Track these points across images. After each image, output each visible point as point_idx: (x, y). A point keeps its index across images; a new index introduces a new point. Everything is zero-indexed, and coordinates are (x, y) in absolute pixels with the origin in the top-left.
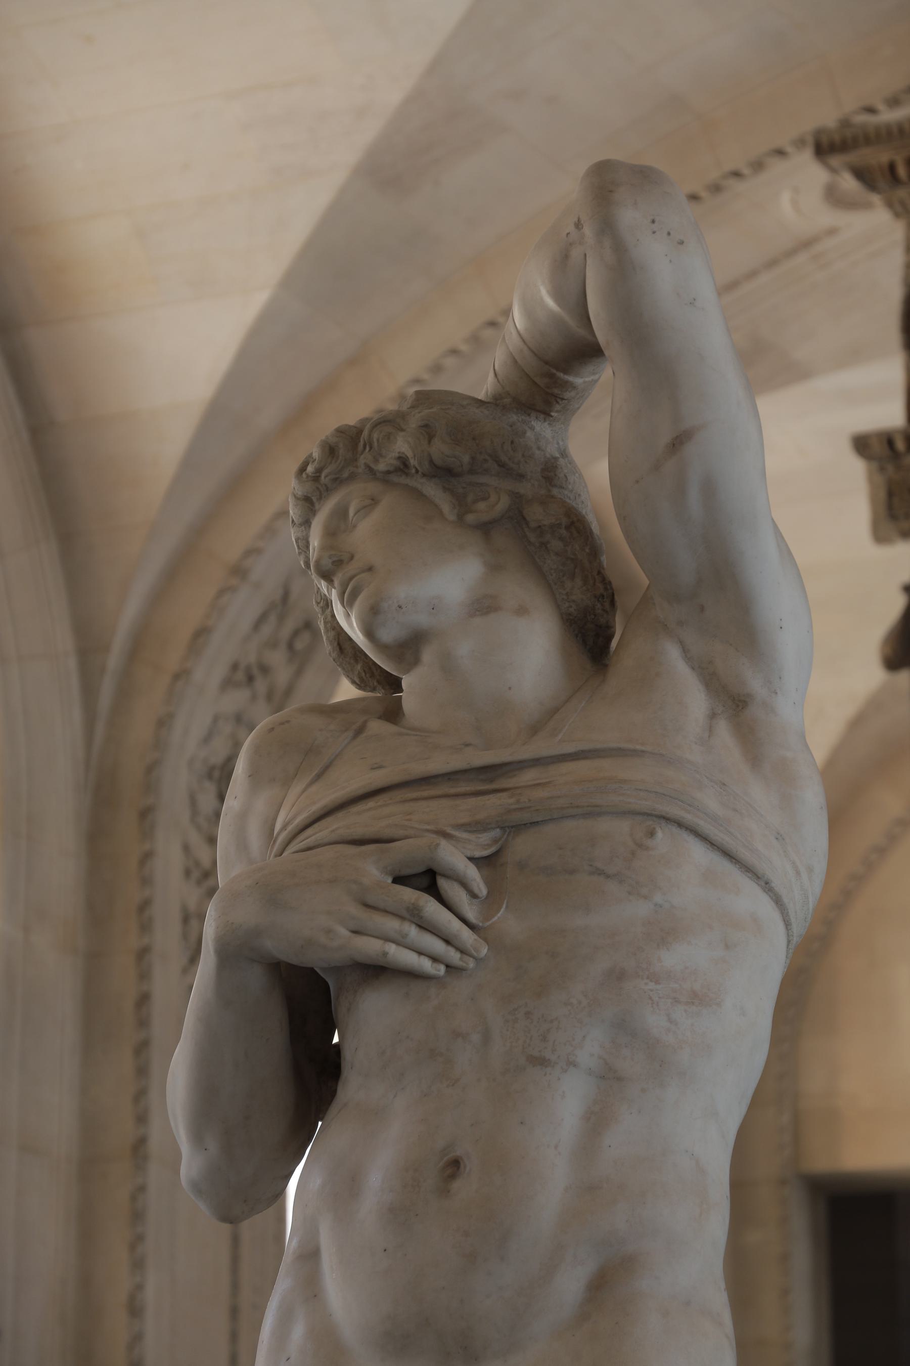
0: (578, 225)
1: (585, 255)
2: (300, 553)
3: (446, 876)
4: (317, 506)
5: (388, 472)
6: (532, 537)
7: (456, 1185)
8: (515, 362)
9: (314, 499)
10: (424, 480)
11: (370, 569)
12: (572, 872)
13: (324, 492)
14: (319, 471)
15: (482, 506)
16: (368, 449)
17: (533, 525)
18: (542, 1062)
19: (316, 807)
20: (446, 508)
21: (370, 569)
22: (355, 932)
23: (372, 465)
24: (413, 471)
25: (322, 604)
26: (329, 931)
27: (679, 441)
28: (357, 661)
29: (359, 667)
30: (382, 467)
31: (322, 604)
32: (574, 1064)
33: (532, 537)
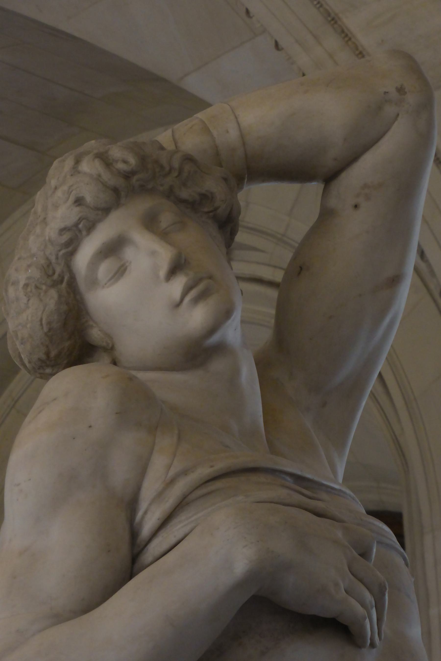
0: (401, 90)
1: (398, 115)
2: (62, 231)
8: (217, 154)
9: (123, 194)
11: (210, 277)
14: (133, 173)
21: (210, 277)
22: (346, 591)
24: (206, 210)
25: (56, 277)
26: (336, 585)
27: (395, 281)
29: (67, 344)
30: (184, 194)
31: (56, 277)
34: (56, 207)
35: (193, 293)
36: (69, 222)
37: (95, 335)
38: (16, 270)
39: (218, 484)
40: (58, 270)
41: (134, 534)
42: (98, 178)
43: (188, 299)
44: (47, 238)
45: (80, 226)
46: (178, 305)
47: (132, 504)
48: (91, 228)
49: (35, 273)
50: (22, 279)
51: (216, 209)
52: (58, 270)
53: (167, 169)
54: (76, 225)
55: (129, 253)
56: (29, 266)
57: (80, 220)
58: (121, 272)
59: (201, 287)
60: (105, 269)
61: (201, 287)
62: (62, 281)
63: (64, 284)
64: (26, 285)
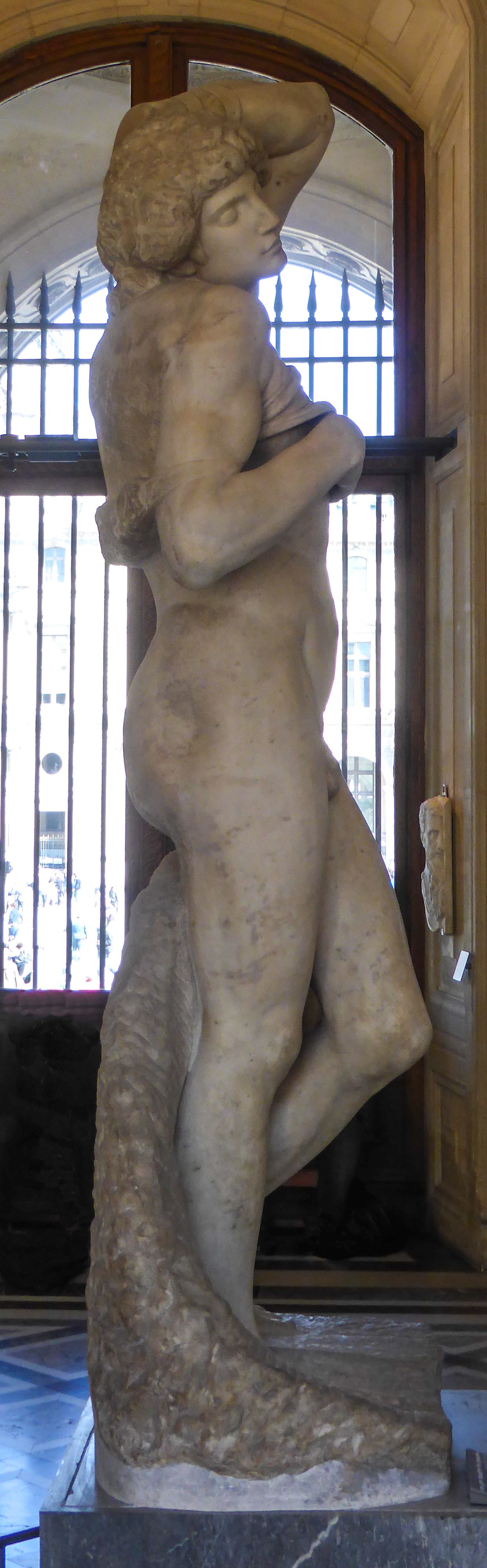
34: (209, 162)
36: (218, 178)
38: (165, 195)
40: (197, 205)
42: (240, 152)
44: (198, 182)
45: (224, 182)
49: (184, 203)
50: (172, 203)
52: (197, 205)
54: (222, 180)
55: (242, 208)
56: (179, 197)
60: (226, 215)
64: (174, 209)
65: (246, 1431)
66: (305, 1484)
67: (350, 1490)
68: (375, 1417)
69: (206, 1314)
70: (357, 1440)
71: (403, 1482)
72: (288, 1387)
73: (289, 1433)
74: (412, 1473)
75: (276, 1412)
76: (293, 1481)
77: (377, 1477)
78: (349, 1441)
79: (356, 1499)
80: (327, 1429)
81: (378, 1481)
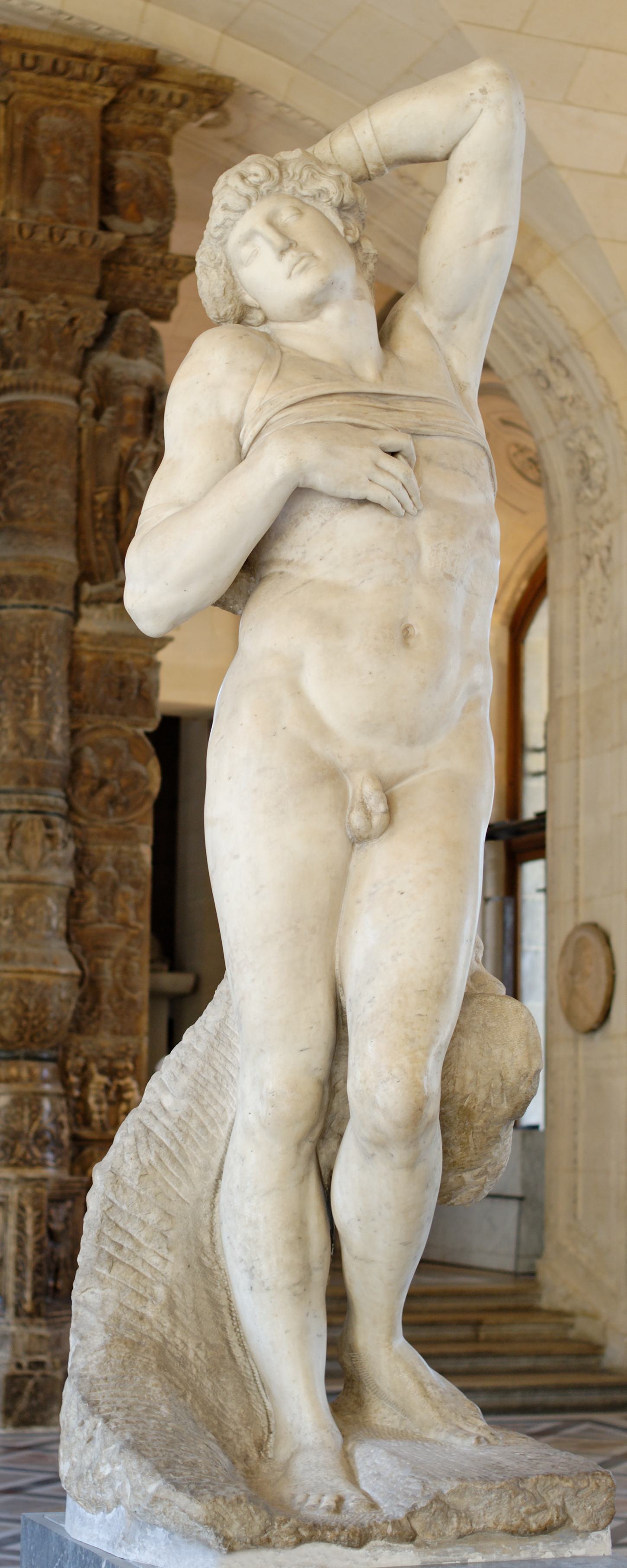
3: (405, 457)
4: (254, 203)
5: (305, 196)
6: (361, 258)
7: (412, 641)
8: (360, 149)
9: (253, 199)
10: (329, 208)
12: (456, 470)
13: (259, 196)
15: (351, 232)
16: (297, 178)
17: (365, 251)
18: (450, 577)
19: (300, 397)
20: (341, 229)
23: (298, 189)
24: (325, 200)
25: (216, 261)
28: (230, 303)
29: (230, 307)
31: (216, 261)
32: (462, 582)
33: (361, 258)
35: (298, 268)
37: (248, 299)
39: (294, 410)
40: (218, 255)
41: (241, 447)
43: (293, 272)
46: (290, 276)
47: (238, 428)
48: (234, 223)
51: (331, 200)
53: (291, 174)
57: (225, 220)
58: (256, 253)
59: (303, 263)
61: (303, 263)
62: (221, 263)
63: (223, 266)
65: (75, 1460)
66: (109, 1525)
67: (127, 1539)
68: (134, 1464)
69: (78, 1342)
70: (128, 1487)
71: (167, 1544)
72: (88, 1419)
73: (90, 1468)
74: (176, 1537)
75: (85, 1442)
76: (105, 1520)
77: (146, 1532)
78: (122, 1487)
79: (130, 1550)
80: (106, 1470)
81: (146, 1537)
